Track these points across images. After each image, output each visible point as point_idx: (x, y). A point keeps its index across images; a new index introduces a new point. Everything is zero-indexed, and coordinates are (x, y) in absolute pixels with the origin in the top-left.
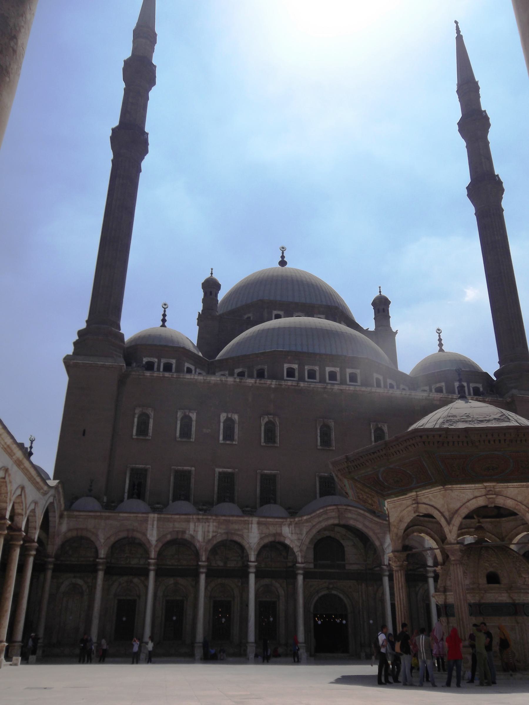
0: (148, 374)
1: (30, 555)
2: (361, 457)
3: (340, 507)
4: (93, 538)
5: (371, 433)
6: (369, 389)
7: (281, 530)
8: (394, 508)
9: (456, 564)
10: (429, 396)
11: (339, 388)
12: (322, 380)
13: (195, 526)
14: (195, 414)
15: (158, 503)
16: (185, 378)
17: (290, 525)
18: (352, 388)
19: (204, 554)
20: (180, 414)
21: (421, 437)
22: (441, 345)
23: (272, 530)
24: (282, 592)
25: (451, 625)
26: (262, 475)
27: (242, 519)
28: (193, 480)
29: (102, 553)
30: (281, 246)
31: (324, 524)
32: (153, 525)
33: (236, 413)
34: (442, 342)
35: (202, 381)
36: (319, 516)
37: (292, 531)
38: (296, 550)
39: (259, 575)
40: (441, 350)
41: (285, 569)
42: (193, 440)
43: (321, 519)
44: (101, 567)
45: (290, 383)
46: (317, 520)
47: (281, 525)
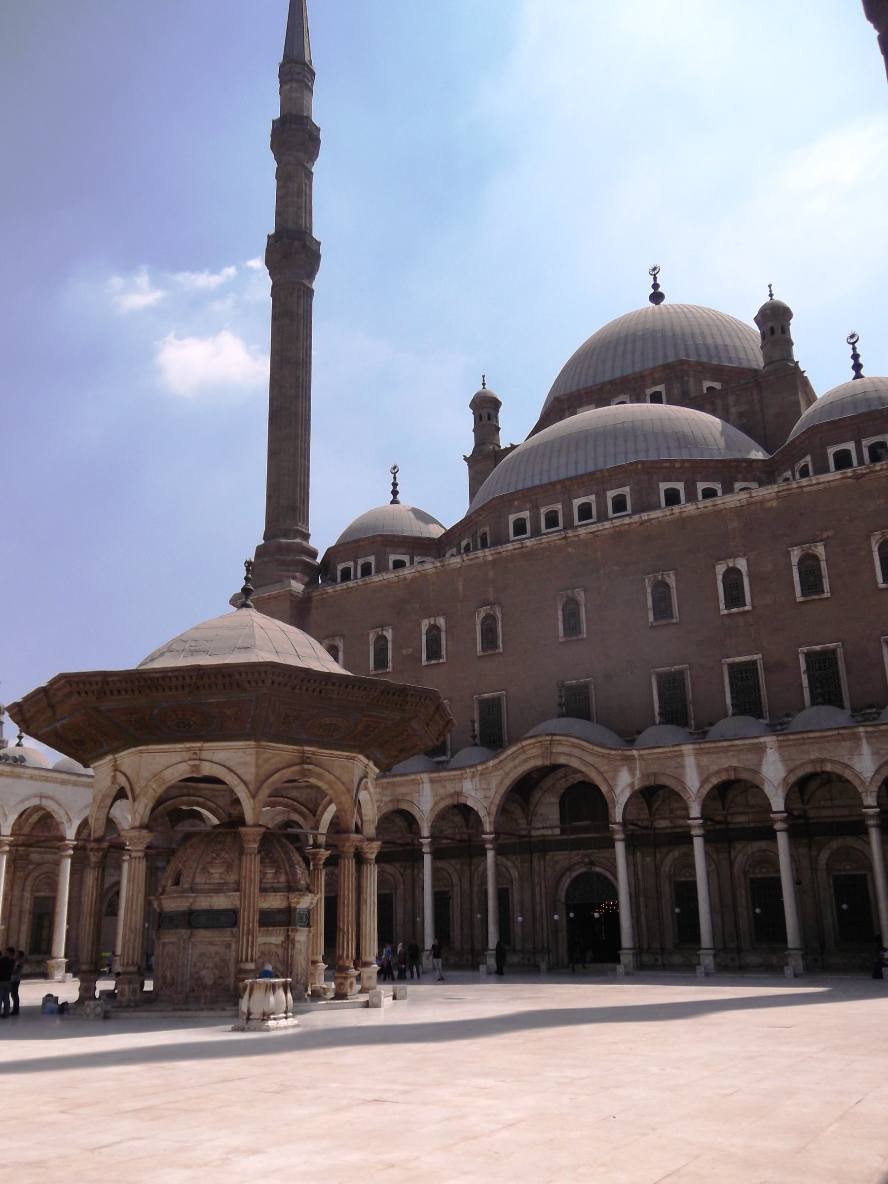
1: (123, 861)
3: (540, 739)
6: (654, 514)
10: (751, 497)
12: (569, 525)
14: (390, 631)
17: (473, 777)
20: (372, 637)
23: (450, 788)
24: (515, 873)
26: (482, 702)
33: (439, 615)
35: (396, 579)
36: (513, 757)
38: (482, 813)
39: (437, 855)
42: (390, 669)
43: (517, 761)
46: (511, 765)
47: (461, 779)
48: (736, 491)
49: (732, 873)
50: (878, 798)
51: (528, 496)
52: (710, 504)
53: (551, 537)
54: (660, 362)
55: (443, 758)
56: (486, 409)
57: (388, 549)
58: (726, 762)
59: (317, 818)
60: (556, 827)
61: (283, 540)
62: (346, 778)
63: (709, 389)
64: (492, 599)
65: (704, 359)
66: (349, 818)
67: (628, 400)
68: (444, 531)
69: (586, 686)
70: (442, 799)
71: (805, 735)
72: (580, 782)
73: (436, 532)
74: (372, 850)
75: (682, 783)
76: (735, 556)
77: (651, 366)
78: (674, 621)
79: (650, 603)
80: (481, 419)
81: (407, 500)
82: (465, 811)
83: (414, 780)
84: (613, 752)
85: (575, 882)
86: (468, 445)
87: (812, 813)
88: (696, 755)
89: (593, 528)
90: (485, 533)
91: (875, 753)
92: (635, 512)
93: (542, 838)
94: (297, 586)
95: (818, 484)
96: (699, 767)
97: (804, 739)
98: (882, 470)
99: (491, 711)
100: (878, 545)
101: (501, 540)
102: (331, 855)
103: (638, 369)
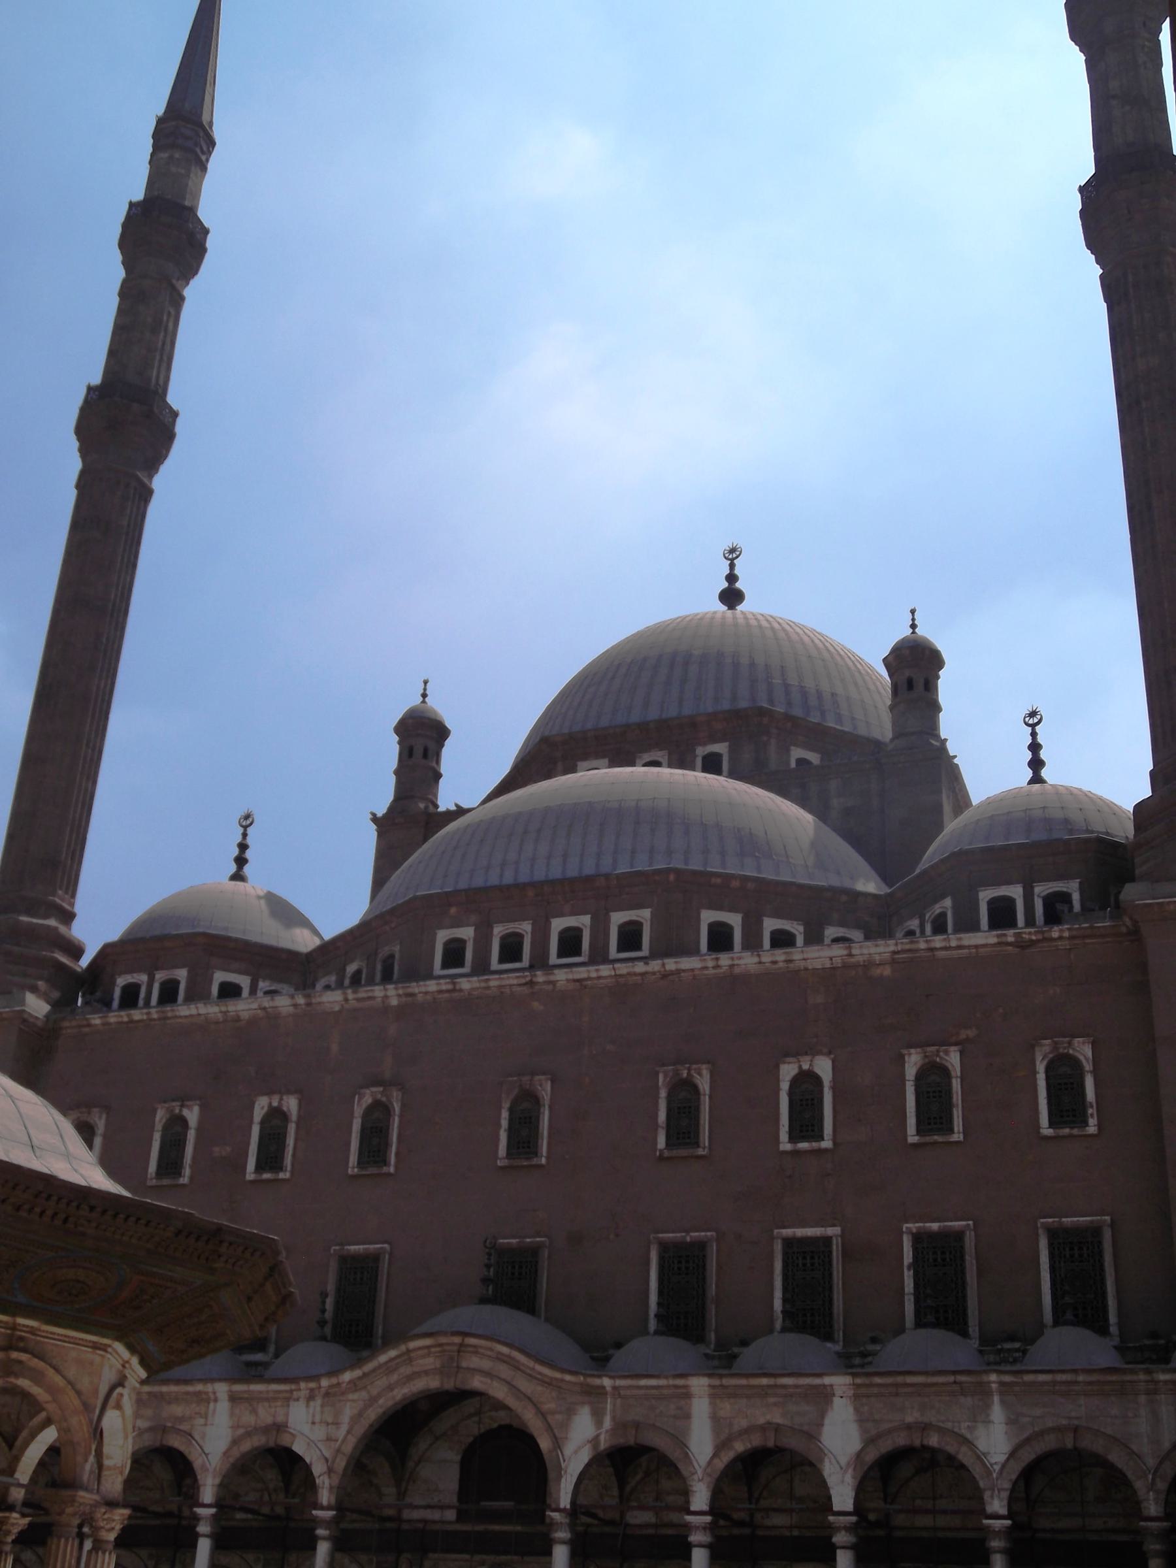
3: (443, 1340)
6: (688, 963)
7: (287, 1415)
11: (570, 977)
12: (540, 962)
14: (196, 1109)
16: (180, 1017)
17: (311, 1398)
20: (161, 1116)
22: (1036, 764)
23: (265, 1415)
27: (190, 1388)
30: (727, 545)
31: (400, 1393)
37: (314, 1416)
38: (318, 1469)
39: (221, 1542)
40: (1037, 779)
42: (184, 1180)
43: (394, 1377)
46: (382, 1383)
47: (288, 1399)
48: (827, 941)
50: (1011, 1501)
51: (477, 902)
52: (782, 958)
53: (506, 979)
54: (726, 706)
55: (259, 1357)
56: (421, 738)
58: (761, 1415)
59: (14, 1452)
60: (449, 1507)
61: (24, 919)
62: (85, 1384)
63: (801, 762)
65: (797, 712)
66: (79, 1459)
67: (664, 761)
68: (318, 942)
69: (535, 1251)
70: (248, 1434)
71: (900, 1379)
73: (303, 942)
74: (114, 1522)
75: (683, 1446)
76: (813, 1051)
77: (710, 710)
78: (700, 1152)
79: (662, 1117)
80: (411, 755)
81: (262, 877)
82: (286, 1462)
83: (200, 1392)
84: (568, 1377)
86: (382, 798)
87: (900, 1520)
88: (713, 1396)
89: (581, 973)
90: (392, 956)
91: (1010, 1422)
92: (655, 954)
93: (421, 1525)
94: (37, 1006)
95: (959, 947)
96: (715, 1419)
97: (896, 1385)
98: (1061, 938)
99: (359, 1276)
100: (1045, 1063)
101: (417, 971)
102: (30, 1524)
103: (687, 711)
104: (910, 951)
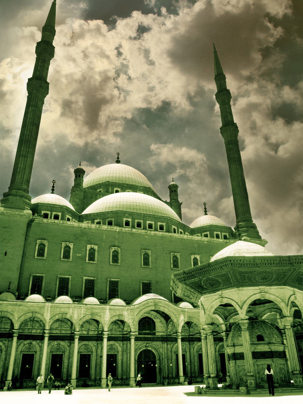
0: (45, 220)
2: (193, 271)
4: (11, 317)
5: (171, 258)
6: (170, 234)
7: (123, 313)
8: (207, 300)
9: (245, 331)
10: (202, 239)
13: (73, 310)
14: (72, 245)
15: (49, 297)
18: (161, 233)
19: (78, 327)
21: (230, 261)
23: (118, 313)
24: (120, 349)
25: (237, 364)
26: (110, 281)
27: (101, 306)
28: (70, 284)
29: (16, 326)
32: (48, 310)
33: (96, 245)
34: (207, 210)
35: (77, 226)
41: (122, 336)
44: (15, 335)
45: (127, 229)
46: (143, 307)
49: (194, 351)
53: (140, 231)
57: (66, 213)
64: (117, 245)
72: (146, 317)
85: (141, 352)
92: (166, 232)
95: (218, 241)
104: (211, 240)
